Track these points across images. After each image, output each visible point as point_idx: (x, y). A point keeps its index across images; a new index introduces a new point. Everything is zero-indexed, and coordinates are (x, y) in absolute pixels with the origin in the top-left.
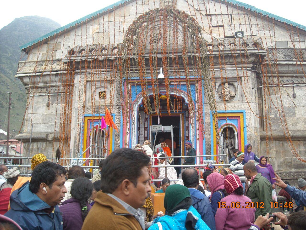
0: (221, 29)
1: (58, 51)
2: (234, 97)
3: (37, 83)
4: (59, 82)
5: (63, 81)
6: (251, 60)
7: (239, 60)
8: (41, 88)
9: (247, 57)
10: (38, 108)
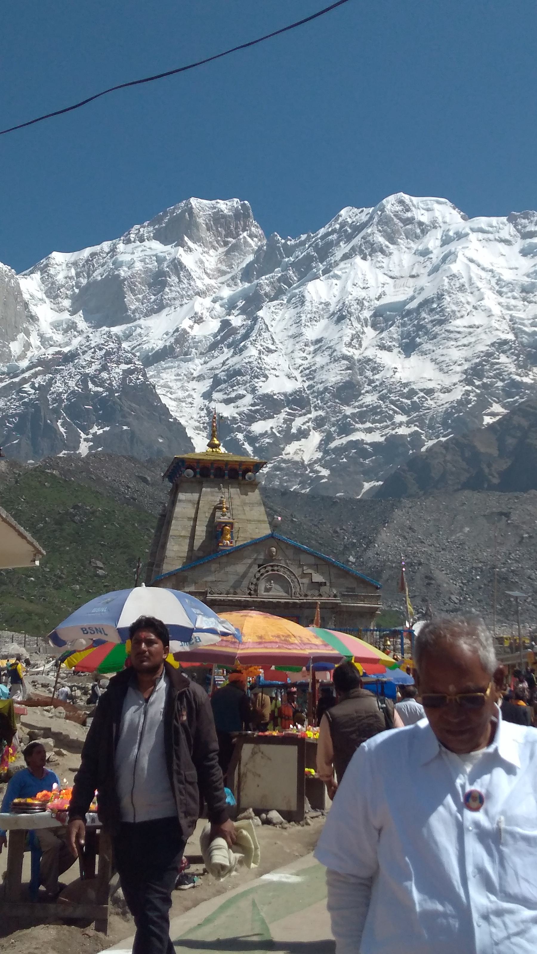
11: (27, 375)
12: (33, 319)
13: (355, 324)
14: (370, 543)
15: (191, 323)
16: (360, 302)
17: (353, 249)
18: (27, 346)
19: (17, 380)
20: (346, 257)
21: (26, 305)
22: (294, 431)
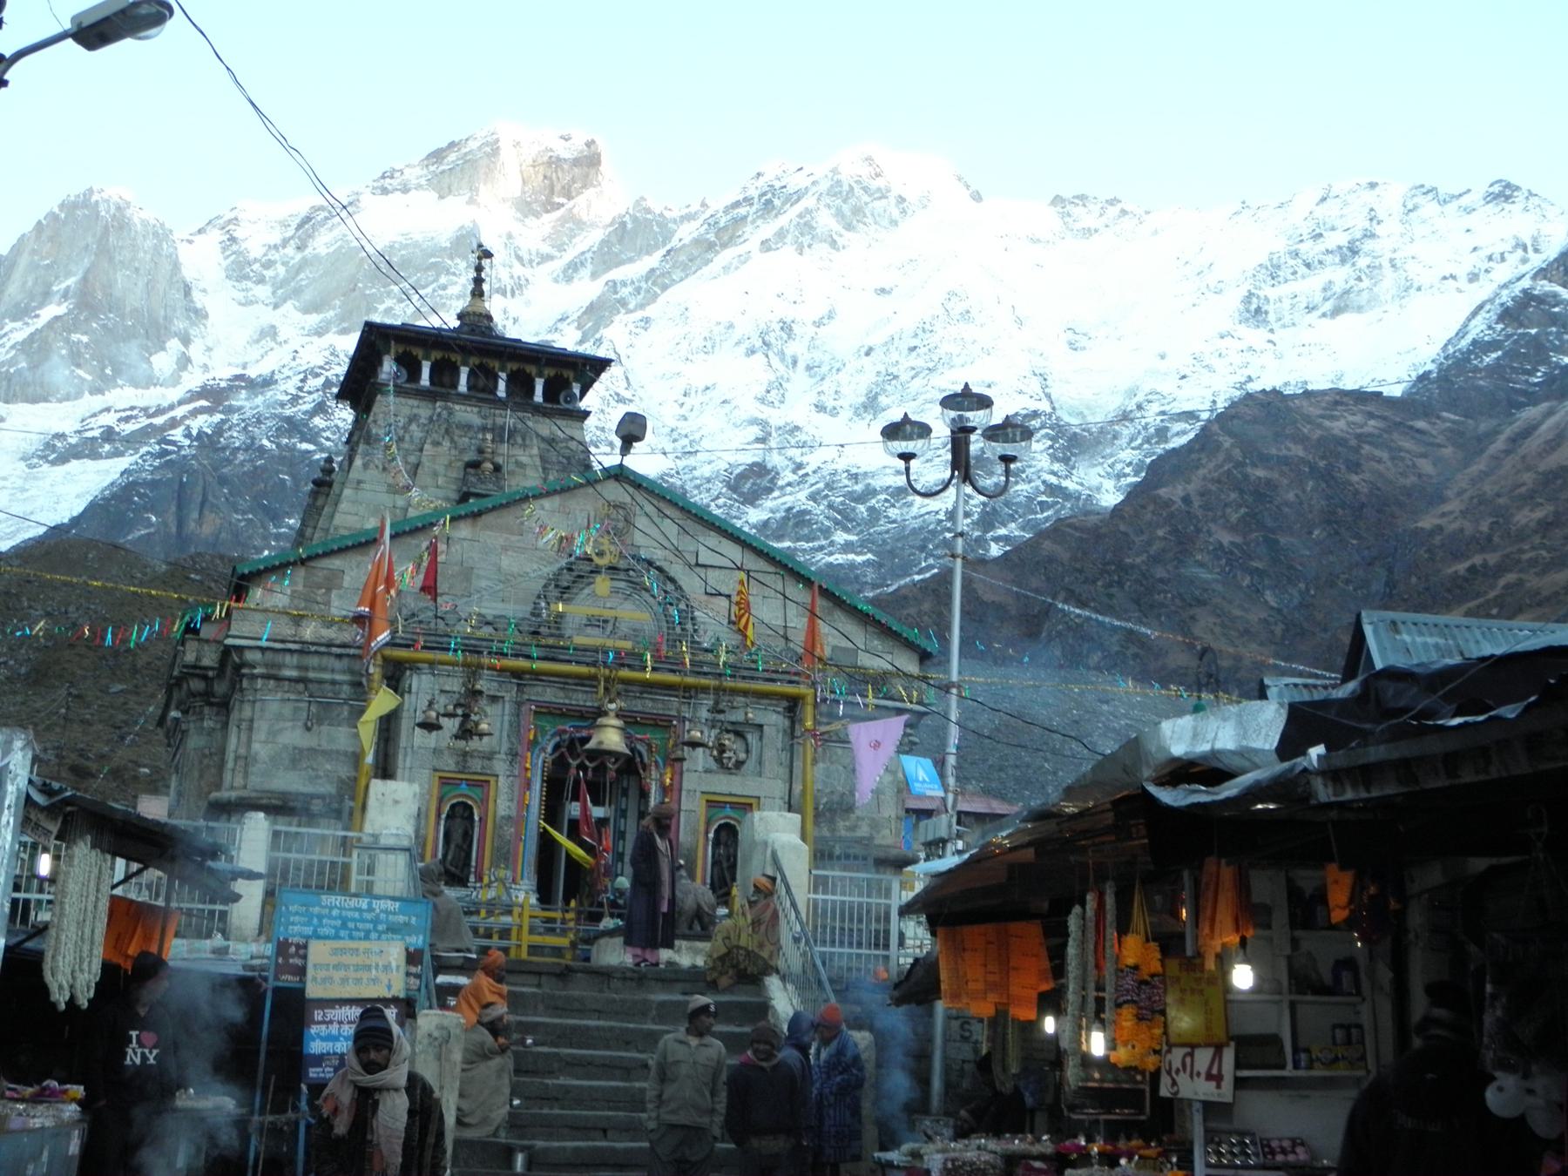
1: (334, 593)
2: (743, 763)
3: (280, 666)
4: (344, 672)
5: (351, 672)
8: (290, 680)
10: (281, 730)
11: (179, 412)
12: (200, 315)
13: (775, 361)
16: (787, 328)
17: (781, 234)
18: (184, 362)
19: (159, 421)
20: (766, 246)
21: (187, 290)
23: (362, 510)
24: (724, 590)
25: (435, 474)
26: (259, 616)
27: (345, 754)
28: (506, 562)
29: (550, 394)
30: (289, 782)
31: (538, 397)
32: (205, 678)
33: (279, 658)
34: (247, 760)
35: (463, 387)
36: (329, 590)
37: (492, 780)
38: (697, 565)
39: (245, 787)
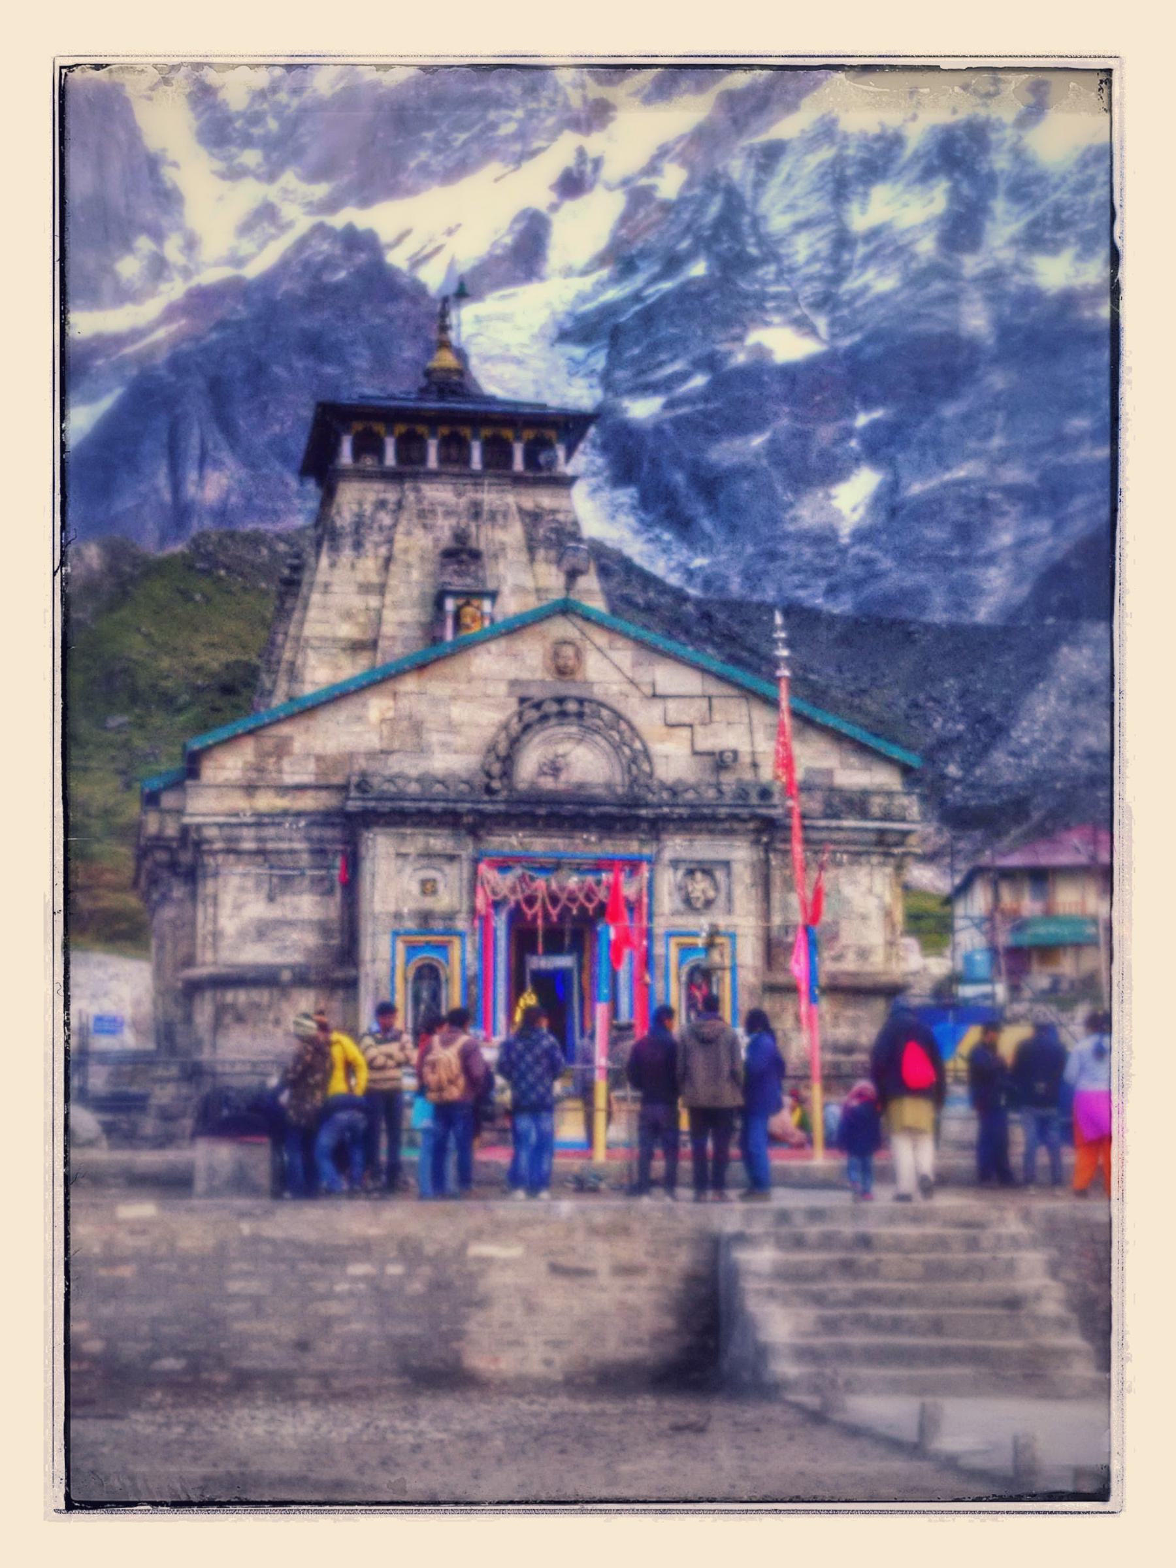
0: (685, 733)
3: (238, 840)
4: (300, 841)
5: (309, 839)
6: (751, 825)
7: (727, 825)
8: (251, 853)
9: (744, 821)
13: (966, 189)
14: (999, 732)
15: (553, 197)
18: (159, 268)
22: (813, 459)
23: (332, 615)
24: (686, 719)
25: (409, 566)
26: (212, 792)
27: (311, 922)
28: (457, 712)
29: (531, 460)
30: (256, 954)
31: (518, 464)
32: (168, 849)
33: (236, 832)
34: (217, 935)
35: (433, 462)
36: (280, 758)
37: (457, 942)
38: (654, 696)
39: (215, 963)
